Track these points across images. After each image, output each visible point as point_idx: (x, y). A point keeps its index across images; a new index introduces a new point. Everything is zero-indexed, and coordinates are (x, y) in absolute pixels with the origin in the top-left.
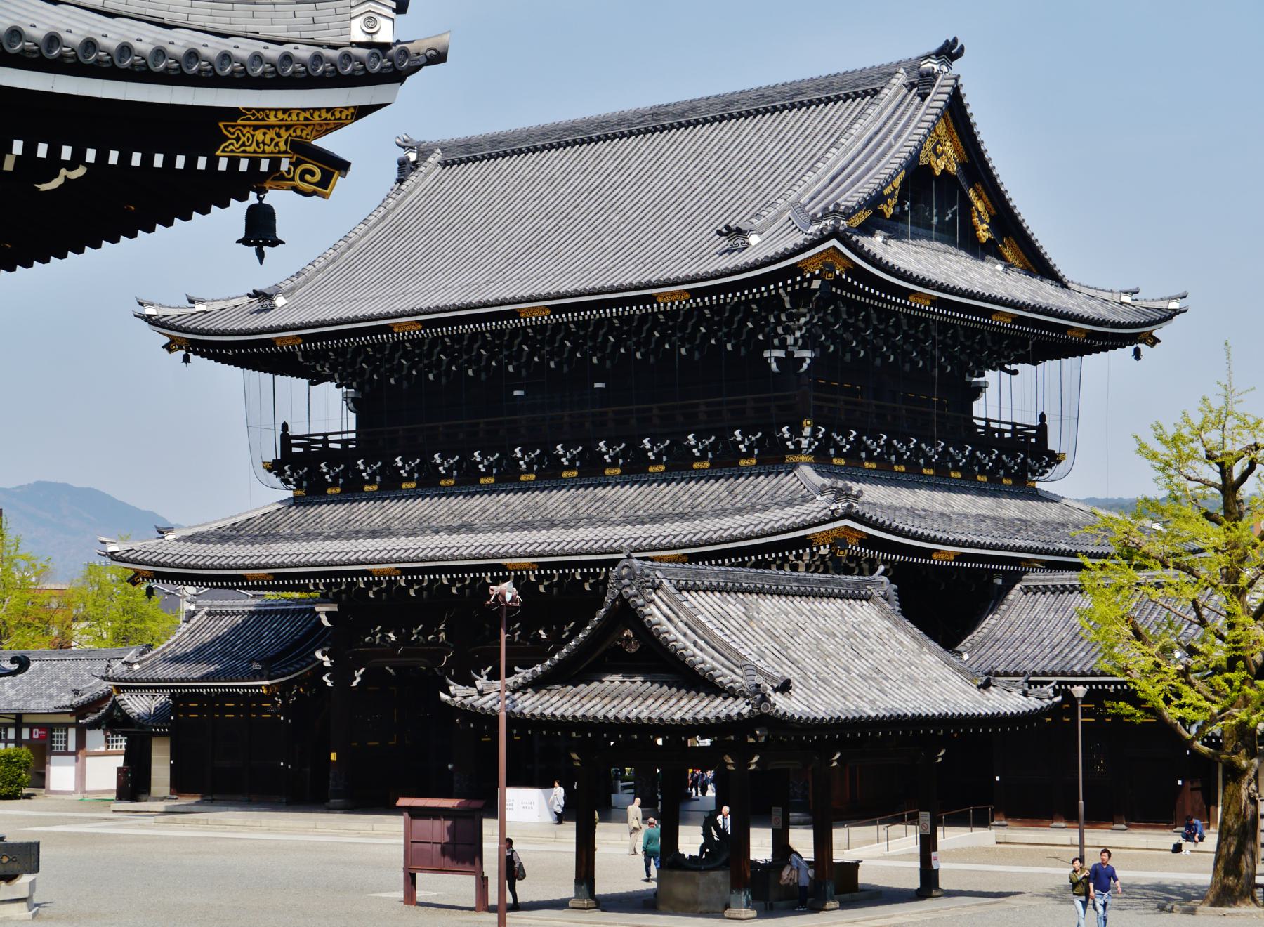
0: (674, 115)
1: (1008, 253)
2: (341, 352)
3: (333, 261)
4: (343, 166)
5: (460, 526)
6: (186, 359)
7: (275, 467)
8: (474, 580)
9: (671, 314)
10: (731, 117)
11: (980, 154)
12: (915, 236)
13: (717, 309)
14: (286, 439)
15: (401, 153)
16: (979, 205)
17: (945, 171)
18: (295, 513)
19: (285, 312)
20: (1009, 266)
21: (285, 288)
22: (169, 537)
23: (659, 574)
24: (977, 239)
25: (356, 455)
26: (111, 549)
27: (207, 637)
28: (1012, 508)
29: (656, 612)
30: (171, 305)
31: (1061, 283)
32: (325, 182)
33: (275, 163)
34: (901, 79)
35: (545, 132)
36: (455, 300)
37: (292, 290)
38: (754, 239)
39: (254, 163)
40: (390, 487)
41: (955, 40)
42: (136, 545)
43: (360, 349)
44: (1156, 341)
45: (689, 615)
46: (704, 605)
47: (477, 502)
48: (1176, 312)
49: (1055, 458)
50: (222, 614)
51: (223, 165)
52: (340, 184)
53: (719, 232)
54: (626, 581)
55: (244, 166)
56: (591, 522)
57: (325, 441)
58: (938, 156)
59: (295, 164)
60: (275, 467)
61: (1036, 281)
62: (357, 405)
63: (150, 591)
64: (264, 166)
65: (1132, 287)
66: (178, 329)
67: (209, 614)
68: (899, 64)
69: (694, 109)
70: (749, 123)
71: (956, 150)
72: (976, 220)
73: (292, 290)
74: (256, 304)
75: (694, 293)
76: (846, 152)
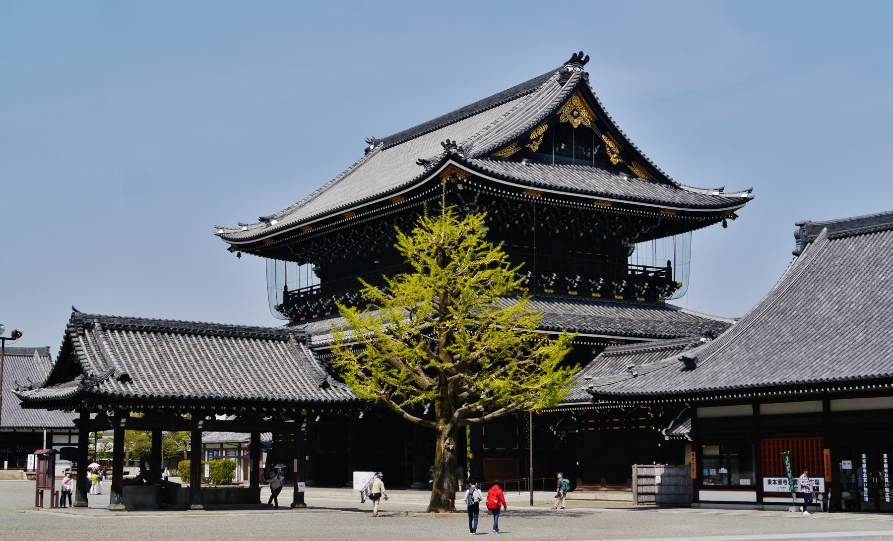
1: (636, 171)
3: (310, 201)
6: (239, 255)
7: (279, 308)
11: (604, 115)
12: (558, 162)
14: (286, 293)
16: (610, 144)
20: (632, 175)
23: (95, 320)
24: (611, 163)
28: (659, 314)
31: (675, 187)
34: (557, 76)
41: (581, 54)
44: (735, 216)
48: (746, 200)
49: (675, 286)
58: (575, 118)
60: (279, 308)
61: (657, 185)
62: (318, 273)
65: (720, 187)
68: (557, 70)
71: (589, 114)
72: (609, 152)
73: (282, 217)
76: (510, 118)
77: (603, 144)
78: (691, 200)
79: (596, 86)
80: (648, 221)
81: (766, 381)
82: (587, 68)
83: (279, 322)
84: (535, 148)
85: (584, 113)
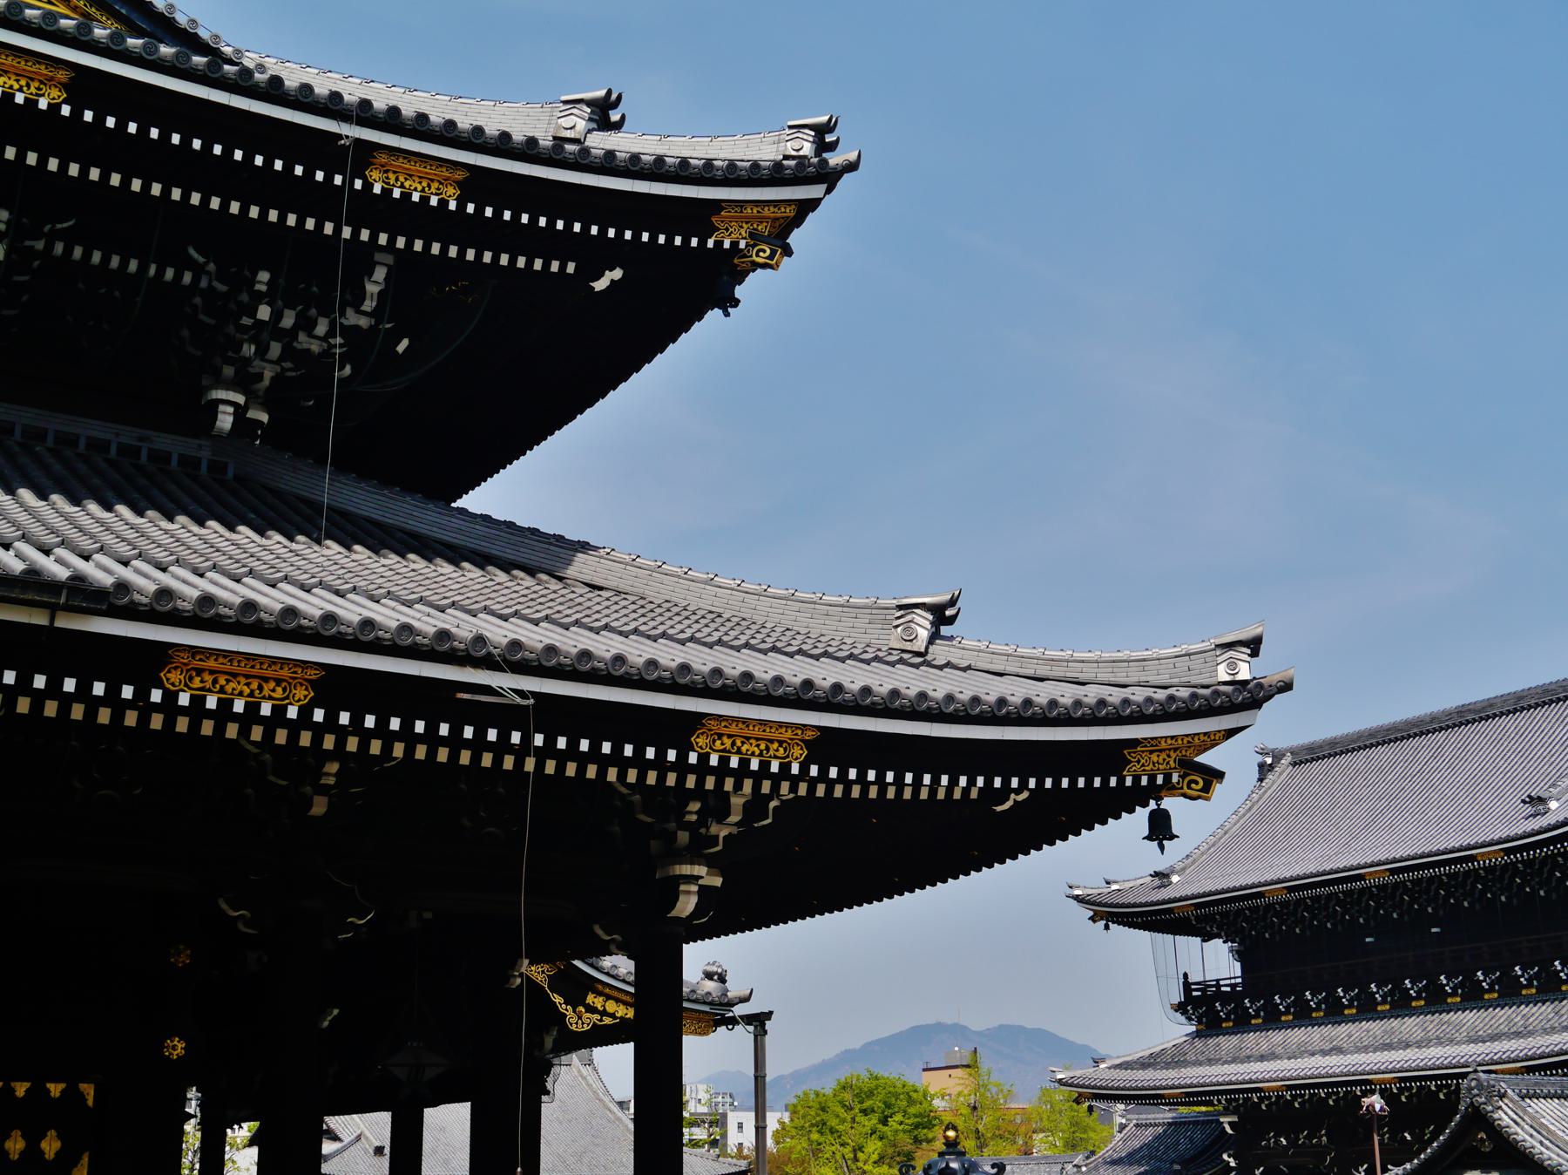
0: (1475, 712)
2: (1225, 915)
4: (1219, 775)
5: (1332, 1050)
6: (1107, 927)
7: (1180, 1008)
8: (1420, 1088)
9: (1490, 870)
10: (1523, 709)
13: (1528, 863)
14: (1187, 985)
15: (1260, 758)
18: (1198, 1043)
19: (1179, 886)
21: (1178, 868)
22: (1102, 1066)
25: (1243, 995)
26: (1060, 1076)
27: (1136, 1144)
29: (1504, 1117)
30: (1092, 886)
32: (1207, 788)
33: (1168, 777)
35: (1372, 733)
36: (1312, 869)
37: (1184, 869)
38: (1553, 805)
39: (1152, 778)
40: (1272, 1020)
42: (1078, 1073)
43: (1240, 912)
45: (1533, 1118)
46: (1547, 1110)
47: (1343, 1029)
50: (1147, 1126)
51: (1129, 782)
52: (1218, 789)
53: (1524, 801)
54: (1475, 1091)
55: (1144, 781)
56: (1440, 1042)
57: (1218, 986)
59: (1183, 777)
60: (1180, 1008)
62: (1241, 956)
63: (1090, 1109)
64: (1160, 780)
66: (1099, 904)
67: (1137, 1125)
69: (1491, 705)
70: (1539, 713)
73: (1184, 869)
74: (1157, 882)
75: (1507, 851)
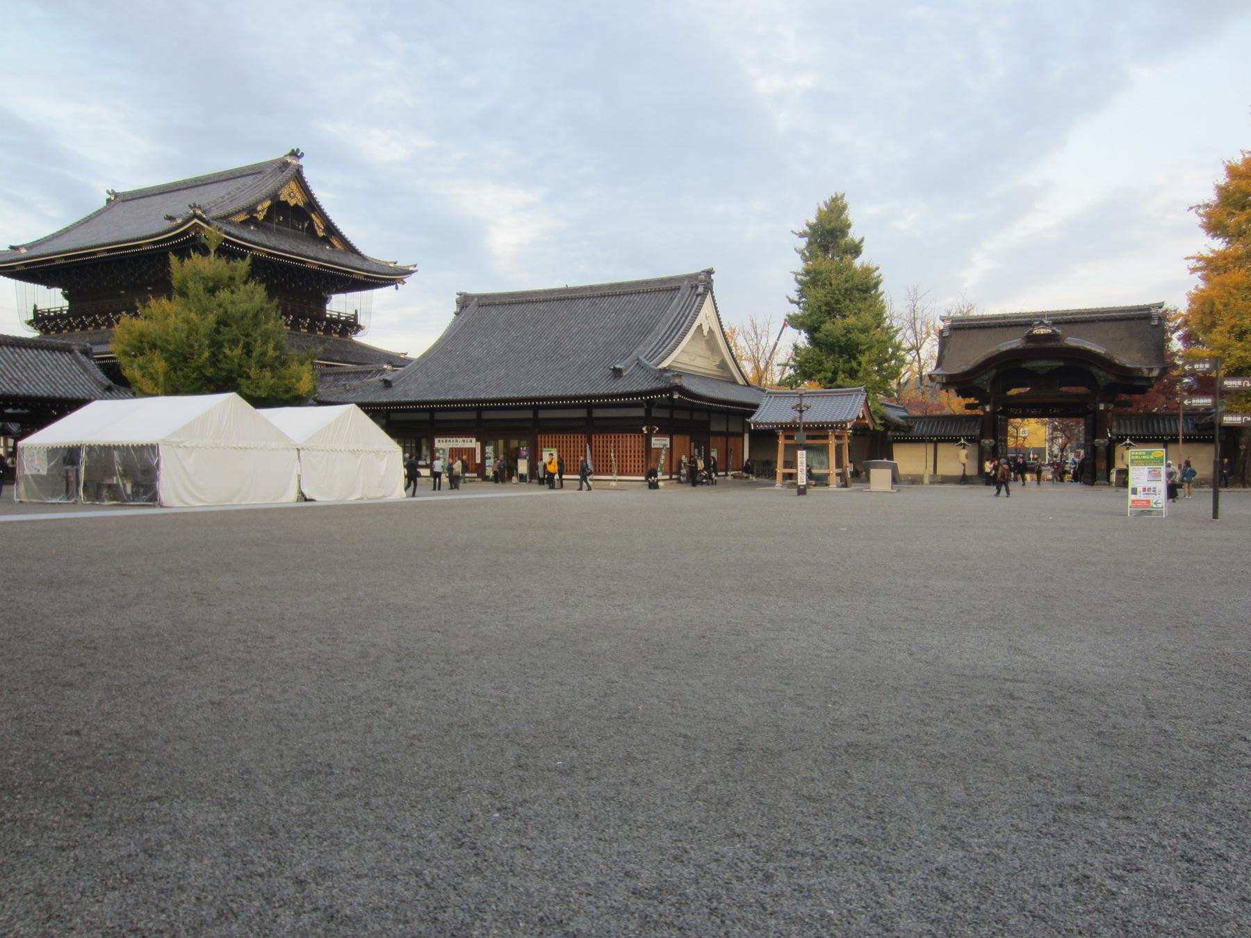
11: (314, 199)
14: (36, 311)
17: (296, 205)
49: (359, 328)
60: (30, 323)
62: (66, 297)
77: (312, 221)
78: (375, 268)
79: (308, 174)
80: (333, 277)
81: (442, 397)
82: (301, 162)
83: (32, 334)
84: (261, 217)
85: (298, 195)
